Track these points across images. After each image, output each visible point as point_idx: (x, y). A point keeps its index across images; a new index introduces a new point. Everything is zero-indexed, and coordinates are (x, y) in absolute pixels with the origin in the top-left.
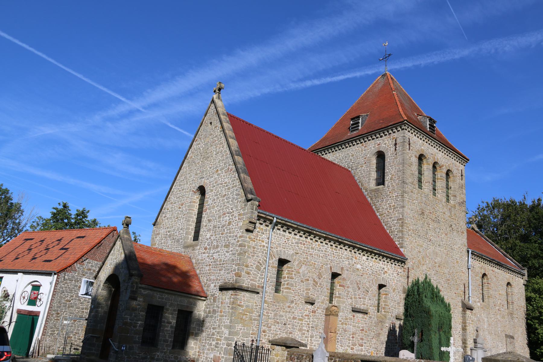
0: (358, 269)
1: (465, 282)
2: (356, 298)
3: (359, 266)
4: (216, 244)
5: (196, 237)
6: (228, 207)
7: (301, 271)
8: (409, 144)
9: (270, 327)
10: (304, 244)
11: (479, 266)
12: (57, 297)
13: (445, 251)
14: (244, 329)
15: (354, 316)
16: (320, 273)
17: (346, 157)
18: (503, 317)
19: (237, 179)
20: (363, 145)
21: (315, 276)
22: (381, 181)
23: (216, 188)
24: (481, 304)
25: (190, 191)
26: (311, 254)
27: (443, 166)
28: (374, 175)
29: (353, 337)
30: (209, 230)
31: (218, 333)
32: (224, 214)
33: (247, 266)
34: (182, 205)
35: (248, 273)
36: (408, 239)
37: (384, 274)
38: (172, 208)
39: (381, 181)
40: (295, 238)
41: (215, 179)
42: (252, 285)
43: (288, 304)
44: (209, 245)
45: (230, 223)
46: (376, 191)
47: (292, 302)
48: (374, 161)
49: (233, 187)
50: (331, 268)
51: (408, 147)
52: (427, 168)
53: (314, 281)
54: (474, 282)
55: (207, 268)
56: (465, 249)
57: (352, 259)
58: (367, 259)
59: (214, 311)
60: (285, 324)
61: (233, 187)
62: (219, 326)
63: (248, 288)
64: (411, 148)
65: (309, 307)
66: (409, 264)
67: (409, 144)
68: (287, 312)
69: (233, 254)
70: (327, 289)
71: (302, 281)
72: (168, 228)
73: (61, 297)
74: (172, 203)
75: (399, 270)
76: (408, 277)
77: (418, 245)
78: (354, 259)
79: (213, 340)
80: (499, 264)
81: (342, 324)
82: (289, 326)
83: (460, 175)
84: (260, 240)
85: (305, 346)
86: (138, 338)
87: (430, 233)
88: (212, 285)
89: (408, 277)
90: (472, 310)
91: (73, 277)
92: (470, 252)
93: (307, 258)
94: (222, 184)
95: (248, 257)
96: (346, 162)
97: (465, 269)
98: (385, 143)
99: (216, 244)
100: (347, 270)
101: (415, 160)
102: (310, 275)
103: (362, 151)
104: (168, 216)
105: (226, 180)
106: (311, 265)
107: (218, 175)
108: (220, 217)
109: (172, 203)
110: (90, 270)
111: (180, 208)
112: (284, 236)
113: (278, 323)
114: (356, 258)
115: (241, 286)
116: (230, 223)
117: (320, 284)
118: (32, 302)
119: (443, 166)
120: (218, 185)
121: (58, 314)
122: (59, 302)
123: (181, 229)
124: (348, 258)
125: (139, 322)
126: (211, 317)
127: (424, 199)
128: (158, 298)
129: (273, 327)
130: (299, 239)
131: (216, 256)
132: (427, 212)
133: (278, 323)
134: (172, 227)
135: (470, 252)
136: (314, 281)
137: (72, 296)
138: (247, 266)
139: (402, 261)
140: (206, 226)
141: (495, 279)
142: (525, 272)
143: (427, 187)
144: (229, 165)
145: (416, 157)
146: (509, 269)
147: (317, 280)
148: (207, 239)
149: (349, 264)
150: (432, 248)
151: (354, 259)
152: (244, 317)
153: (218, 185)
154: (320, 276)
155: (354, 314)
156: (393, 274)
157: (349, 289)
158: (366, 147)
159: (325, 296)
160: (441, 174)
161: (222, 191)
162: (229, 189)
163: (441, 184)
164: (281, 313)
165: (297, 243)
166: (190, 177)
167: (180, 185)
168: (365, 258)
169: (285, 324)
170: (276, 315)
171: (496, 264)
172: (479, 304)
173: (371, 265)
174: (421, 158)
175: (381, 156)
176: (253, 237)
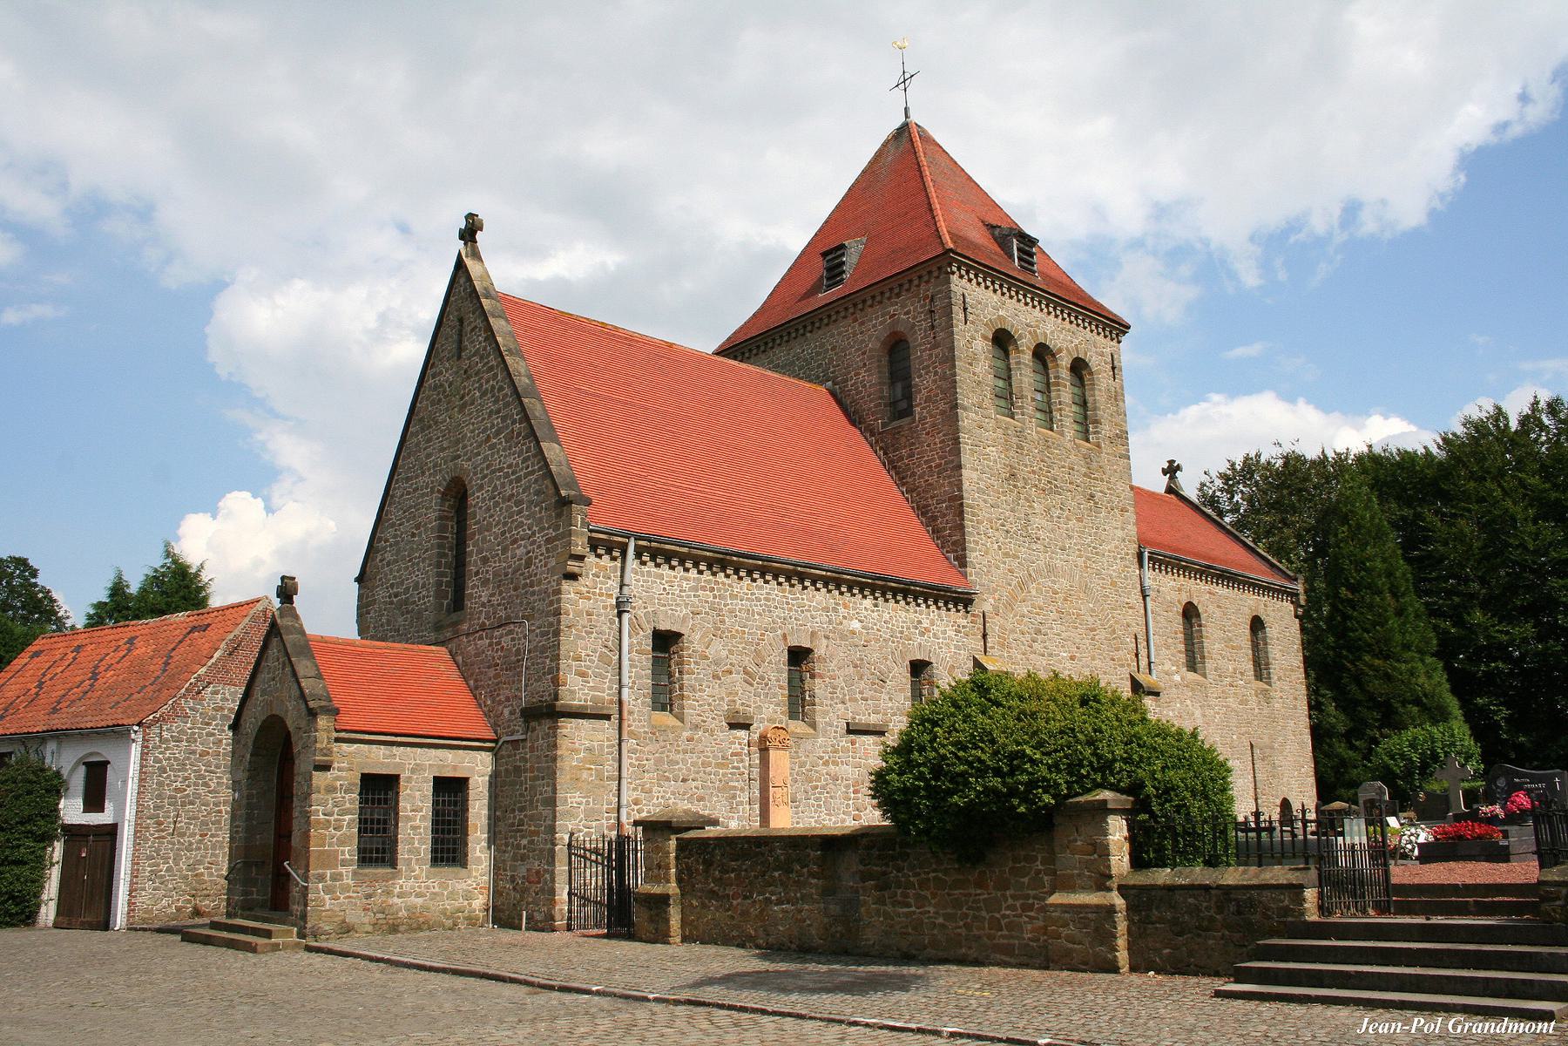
1: (1135, 629)
2: (856, 700)
3: (856, 625)
4: (503, 614)
5: (458, 603)
6: (521, 525)
8: (965, 309)
9: (650, 791)
10: (712, 590)
11: (1171, 588)
12: (152, 783)
13: (1080, 562)
14: (588, 803)
15: (853, 743)
17: (818, 354)
18: (1244, 702)
19: (534, 456)
20: (855, 320)
21: (747, 661)
23: (491, 481)
25: (432, 492)
26: (731, 611)
27: (1060, 350)
29: (855, 792)
30: (485, 582)
31: (532, 818)
32: (515, 541)
33: (578, 659)
34: (418, 527)
35: (583, 675)
36: (977, 543)
37: (922, 634)
38: (395, 536)
40: (687, 579)
41: (486, 459)
42: (594, 698)
43: (686, 734)
44: (488, 618)
45: (529, 563)
47: (697, 727)
49: (526, 475)
50: (785, 636)
51: (961, 316)
53: (746, 672)
54: (1167, 626)
55: (491, 672)
56: (1133, 549)
57: (835, 610)
58: (876, 605)
59: (517, 770)
60: (684, 780)
61: (526, 475)
62: (531, 802)
63: (586, 707)
64: (970, 318)
65: (742, 733)
66: (984, 604)
67: (965, 309)
68: (685, 752)
69: (544, 634)
70: (781, 687)
71: (716, 677)
72: (392, 586)
73: (160, 784)
74: (393, 525)
75: (963, 622)
76: (984, 636)
77: (1006, 555)
78: (841, 609)
79: (523, 837)
80: (1226, 577)
81: (826, 763)
82: (694, 784)
83: (1109, 367)
84: (601, 595)
85: (715, 823)
86: (349, 851)
87: (1037, 521)
88: (506, 712)
89: (984, 636)
90: (1157, 694)
91: (182, 732)
92: (1146, 554)
93: (722, 622)
94: (501, 470)
95: (579, 637)
96: (819, 366)
97: (1136, 598)
98: (906, 312)
99: (503, 614)
100: (827, 638)
102: (733, 659)
103: (855, 334)
104: (388, 556)
105: (510, 460)
106: (733, 637)
107: (492, 447)
108: (505, 550)
109: (393, 525)
110: (222, 708)
111: (413, 535)
113: (668, 779)
114: (845, 607)
115: (571, 706)
116: (529, 563)
117: (762, 678)
118: (94, 801)
119: (1060, 350)
120: (494, 472)
121: (159, 823)
122: (159, 796)
123: (424, 586)
124: (826, 609)
125: (347, 817)
126: (513, 784)
127: (1015, 440)
128: (380, 759)
129: (655, 789)
130: (699, 580)
131: (506, 642)
132: (1023, 472)
133: (668, 779)
134: (402, 583)
135: (1146, 554)
136: (746, 672)
137: (186, 779)
138: (578, 659)
139: (962, 600)
140: (477, 573)
141: (1218, 613)
144: (514, 422)
145: (985, 337)
146: (1254, 586)
147: (752, 668)
148: (483, 605)
149: (830, 622)
151: (841, 609)
152: (585, 775)
153: (494, 472)
154: (759, 658)
155: (853, 737)
156: (944, 632)
157: (835, 682)
158: (862, 323)
159: (777, 705)
161: (503, 485)
162: (518, 480)
164: (673, 756)
165: (695, 589)
166: (429, 456)
167: (408, 479)
168: (868, 602)
169: (684, 780)
170: (659, 762)
171: (1219, 577)
172: (1177, 678)
173: (886, 616)
174: (1002, 340)
176: (584, 590)
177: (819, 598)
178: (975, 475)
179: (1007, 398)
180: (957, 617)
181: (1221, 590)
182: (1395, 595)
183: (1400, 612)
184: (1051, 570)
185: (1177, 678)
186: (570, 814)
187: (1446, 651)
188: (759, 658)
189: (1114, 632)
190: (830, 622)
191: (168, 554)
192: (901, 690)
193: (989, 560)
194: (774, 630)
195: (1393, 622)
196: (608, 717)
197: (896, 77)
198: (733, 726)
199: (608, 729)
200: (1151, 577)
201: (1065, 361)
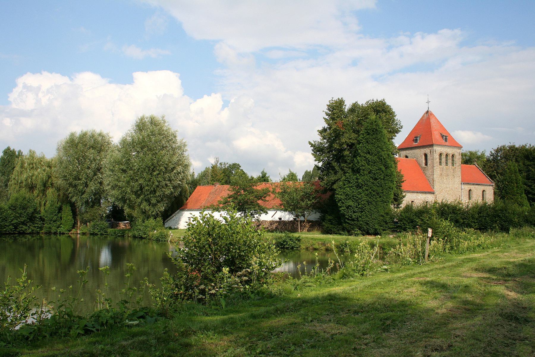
11: (467, 187)
22: (426, 164)
28: (424, 161)
39: (426, 164)
46: (425, 168)
48: (424, 156)
52: (443, 157)
66: (436, 193)
97: (460, 190)
98: (427, 150)
101: (438, 157)
142: (494, 184)
143: (444, 164)
160: (450, 157)
163: (450, 161)
175: (426, 155)
177: (415, 194)
179: (440, 163)
180: (432, 195)
181: (477, 187)
182: (517, 184)
183: (517, 187)
184: (446, 187)
187: (527, 193)
191: (290, 171)
193: (437, 188)
195: (515, 189)
197: (427, 101)
200: (463, 186)
201: (451, 155)
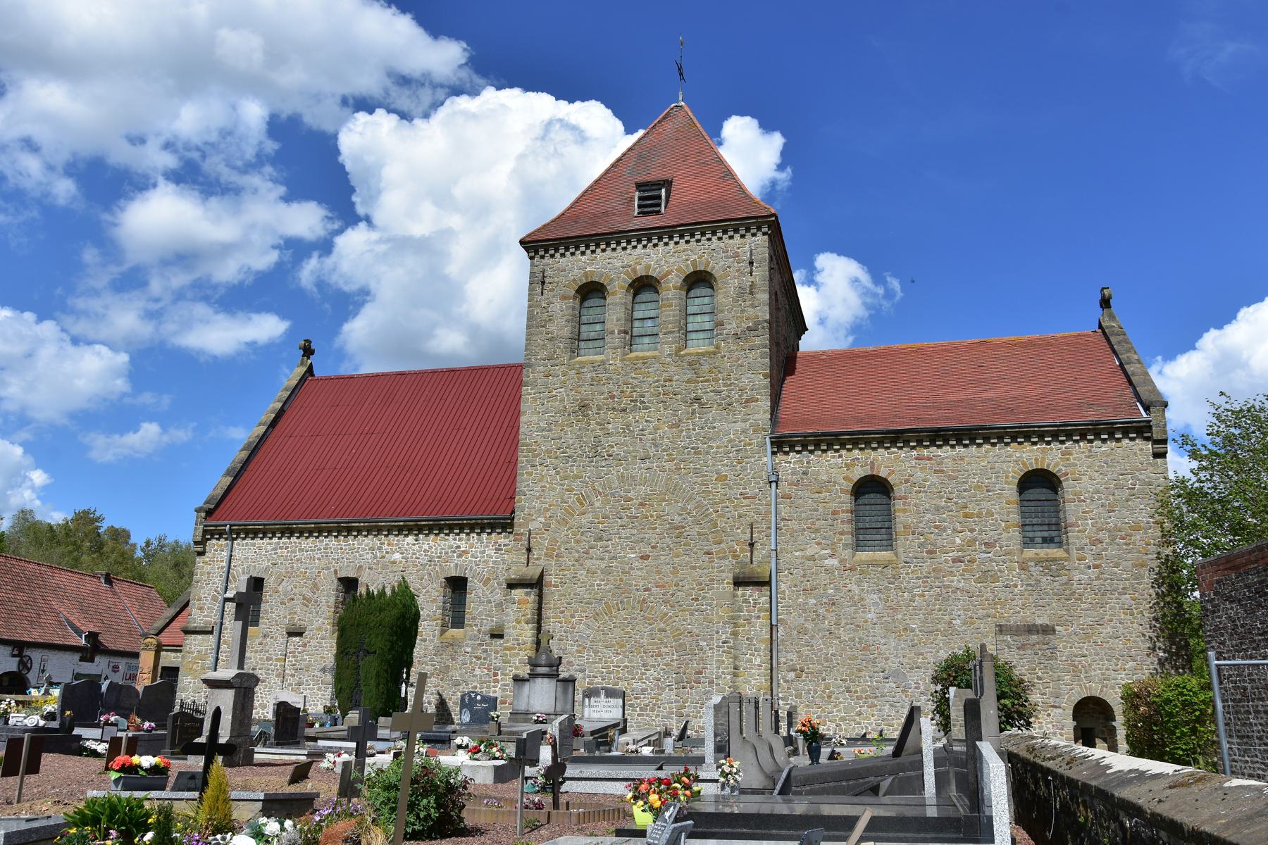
0: (394, 562)
3: (397, 556)
7: (280, 589)
16: (315, 585)
24: (842, 561)
35: (201, 609)
37: (460, 556)
50: (336, 572)
57: (380, 548)
76: (529, 550)
89: (529, 550)
112: (254, 545)
147: (309, 595)
150: (615, 472)
154: (315, 587)
165: (275, 549)
168: (411, 539)
173: (426, 547)
178: (535, 418)
185: (829, 562)
186: (184, 689)
188: (315, 587)
189: (715, 525)
190: (375, 557)
192: (434, 601)
194: (328, 568)
196: (211, 633)
198: (290, 634)
199: (212, 639)
